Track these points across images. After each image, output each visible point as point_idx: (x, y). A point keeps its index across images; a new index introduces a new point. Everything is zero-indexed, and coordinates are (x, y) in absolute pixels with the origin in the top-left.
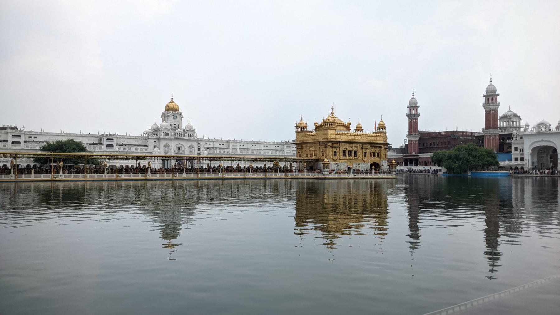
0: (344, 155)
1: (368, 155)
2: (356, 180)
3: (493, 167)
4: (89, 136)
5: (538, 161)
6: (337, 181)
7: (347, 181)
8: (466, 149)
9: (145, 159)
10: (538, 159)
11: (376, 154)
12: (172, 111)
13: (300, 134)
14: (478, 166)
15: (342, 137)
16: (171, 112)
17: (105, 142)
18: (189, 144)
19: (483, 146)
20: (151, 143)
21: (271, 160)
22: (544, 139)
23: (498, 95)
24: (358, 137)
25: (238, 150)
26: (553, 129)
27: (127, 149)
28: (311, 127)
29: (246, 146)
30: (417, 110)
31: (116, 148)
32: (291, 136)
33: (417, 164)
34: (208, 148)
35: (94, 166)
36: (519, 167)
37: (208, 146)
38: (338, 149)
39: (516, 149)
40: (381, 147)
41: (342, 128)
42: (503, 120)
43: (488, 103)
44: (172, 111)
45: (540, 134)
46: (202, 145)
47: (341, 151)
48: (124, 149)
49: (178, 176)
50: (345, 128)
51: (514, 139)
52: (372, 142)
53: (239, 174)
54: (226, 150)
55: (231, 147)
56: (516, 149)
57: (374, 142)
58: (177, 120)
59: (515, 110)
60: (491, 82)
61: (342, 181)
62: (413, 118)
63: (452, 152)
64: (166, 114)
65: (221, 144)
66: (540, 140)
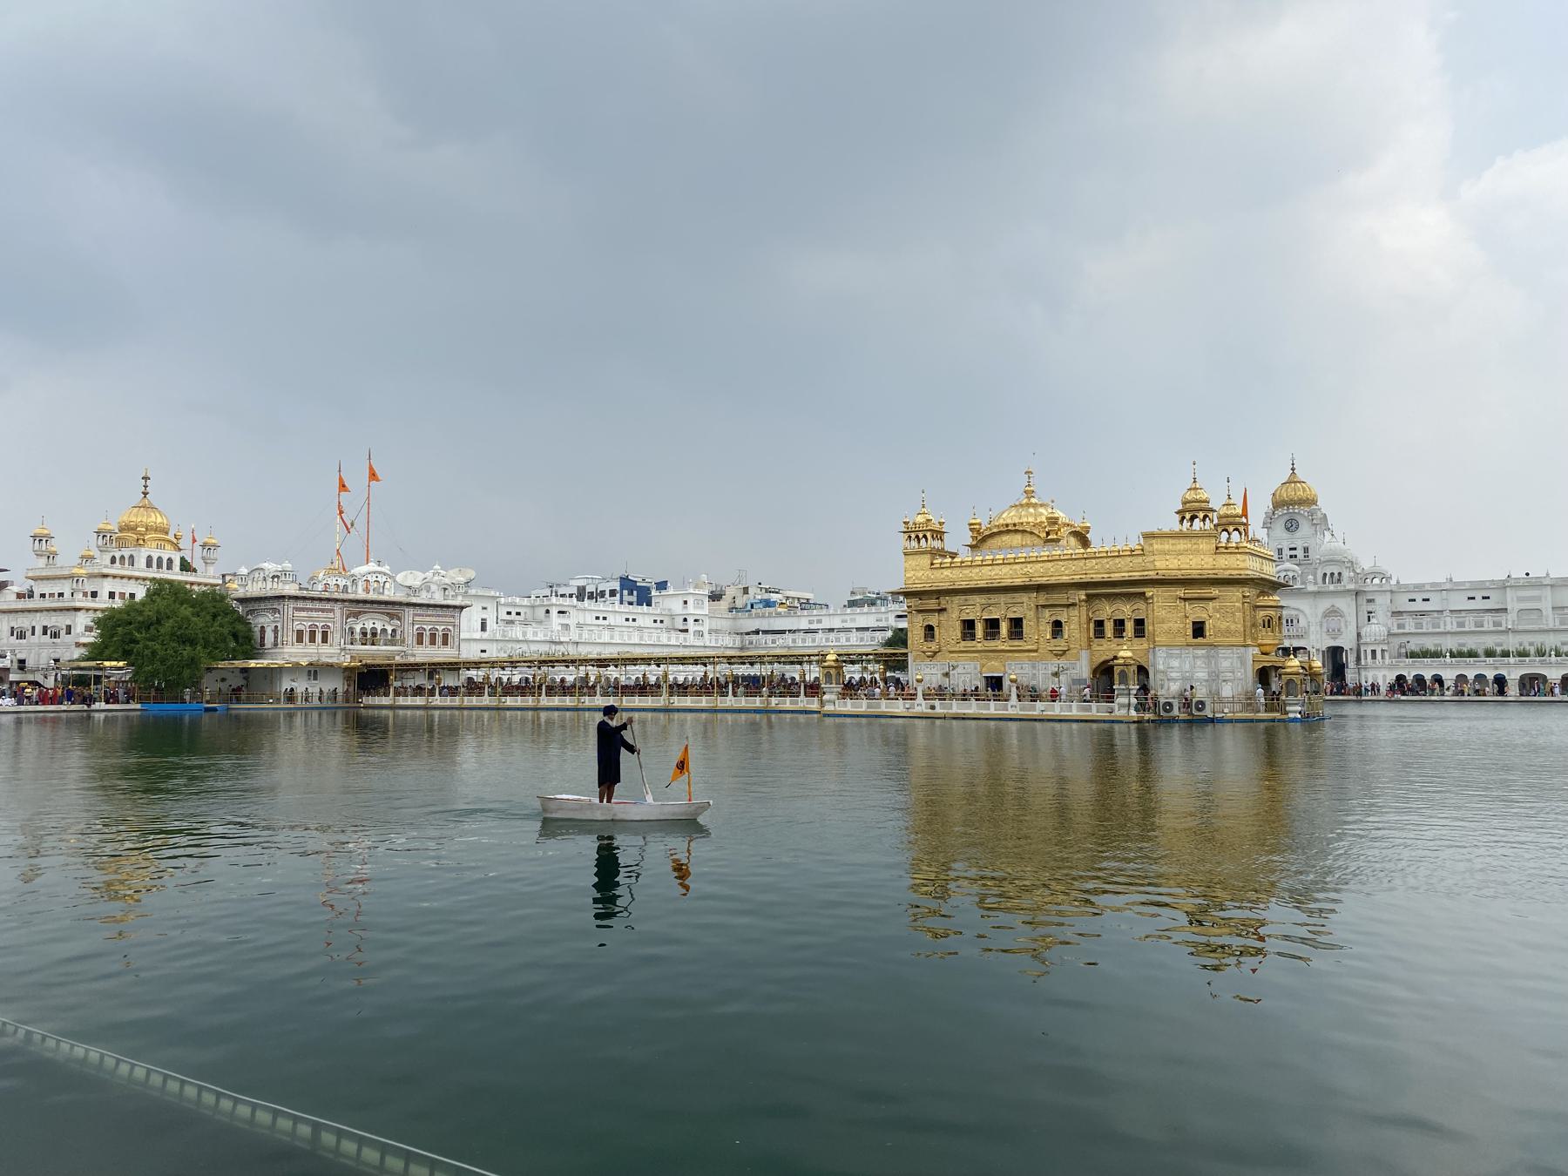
2: (938, 722)
6: (864, 720)
7: (900, 721)
16: (1279, 512)
18: (1325, 604)
24: (1029, 568)
25: (1548, 611)
34: (1423, 614)
37: (1419, 606)
38: (943, 617)
41: (1017, 539)
50: (1028, 539)
52: (1086, 579)
54: (1488, 620)
55: (1513, 605)
57: (1097, 578)
58: (1298, 534)
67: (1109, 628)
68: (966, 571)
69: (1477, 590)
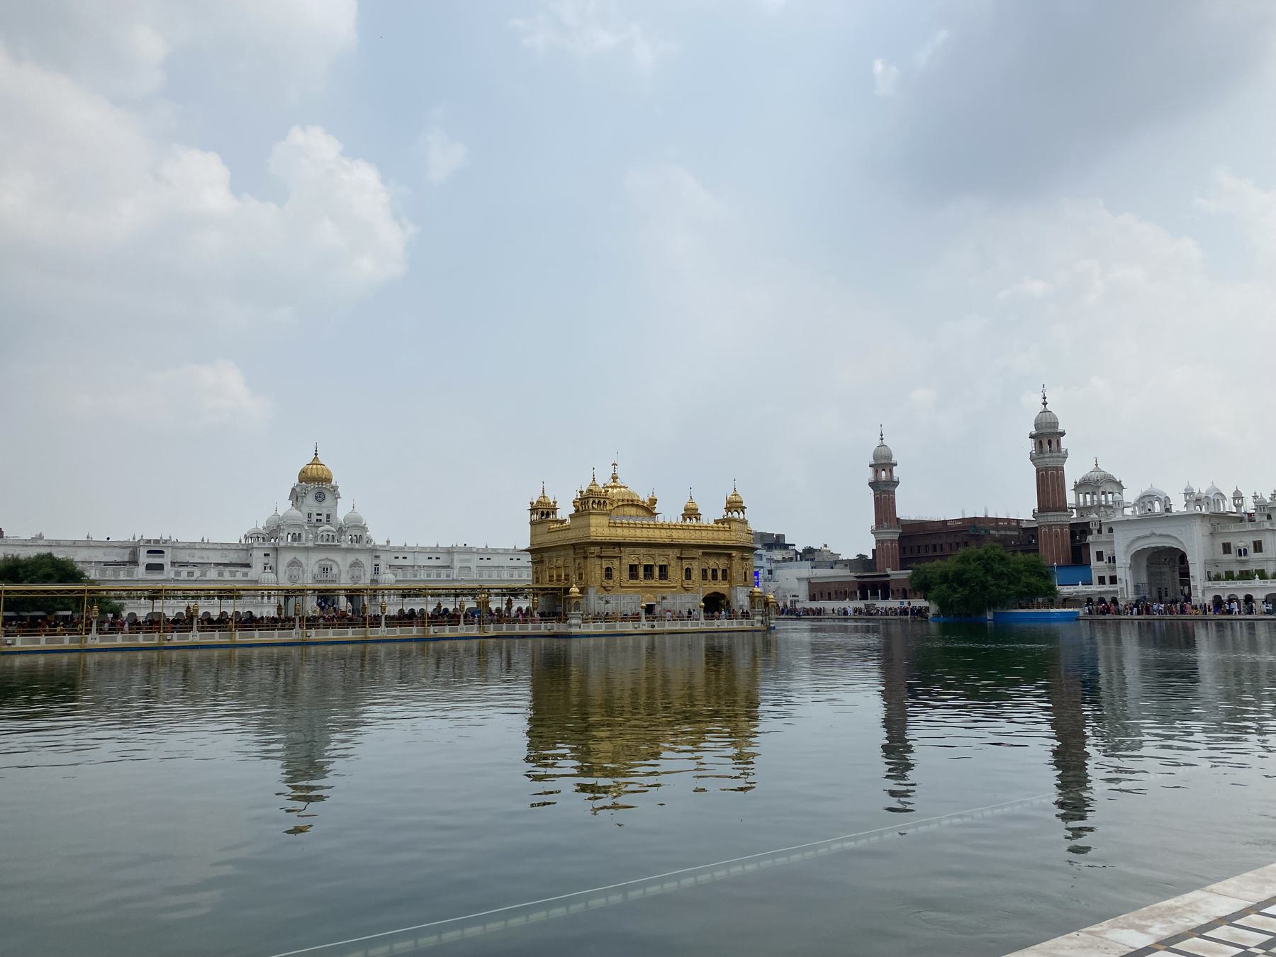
0: (705, 577)
1: (696, 574)
3: (1040, 600)
4: (108, 545)
5: (1150, 583)
6: (603, 640)
7: (631, 638)
8: (979, 558)
9: (239, 597)
10: (1151, 575)
11: (720, 573)
12: (315, 484)
13: (540, 529)
14: (1008, 597)
15: (626, 532)
16: (311, 486)
17: (144, 559)
18: (351, 558)
19: (1037, 550)
20: (258, 559)
21: (472, 592)
22: (1158, 532)
23: (1063, 434)
25: (474, 569)
26: (1178, 506)
27: (197, 573)
28: (565, 511)
29: (496, 561)
30: (891, 471)
31: (169, 572)
32: (517, 534)
33: (885, 597)
34: (400, 567)
35: (110, 615)
36: (1108, 600)
37: (400, 562)
38: (616, 562)
39: (1100, 556)
40: (730, 556)
41: (633, 511)
42: (1084, 489)
43: (1041, 452)
44: (315, 484)
45: (1148, 518)
46: (385, 560)
47: (626, 568)
48: (190, 574)
49: (316, 634)
50: (641, 512)
51: (1095, 532)
52: (705, 542)
53: (350, 630)
54: (444, 572)
55: (457, 564)
56: (1100, 556)
57: (711, 542)
58: (324, 504)
59: (1108, 468)
60: (1045, 404)
61: (618, 640)
62: (884, 491)
63: (950, 565)
64: (298, 489)
65: (434, 556)
66: (1147, 532)
67: (710, 573)
68: (632, 531)
69: (434, 552)
